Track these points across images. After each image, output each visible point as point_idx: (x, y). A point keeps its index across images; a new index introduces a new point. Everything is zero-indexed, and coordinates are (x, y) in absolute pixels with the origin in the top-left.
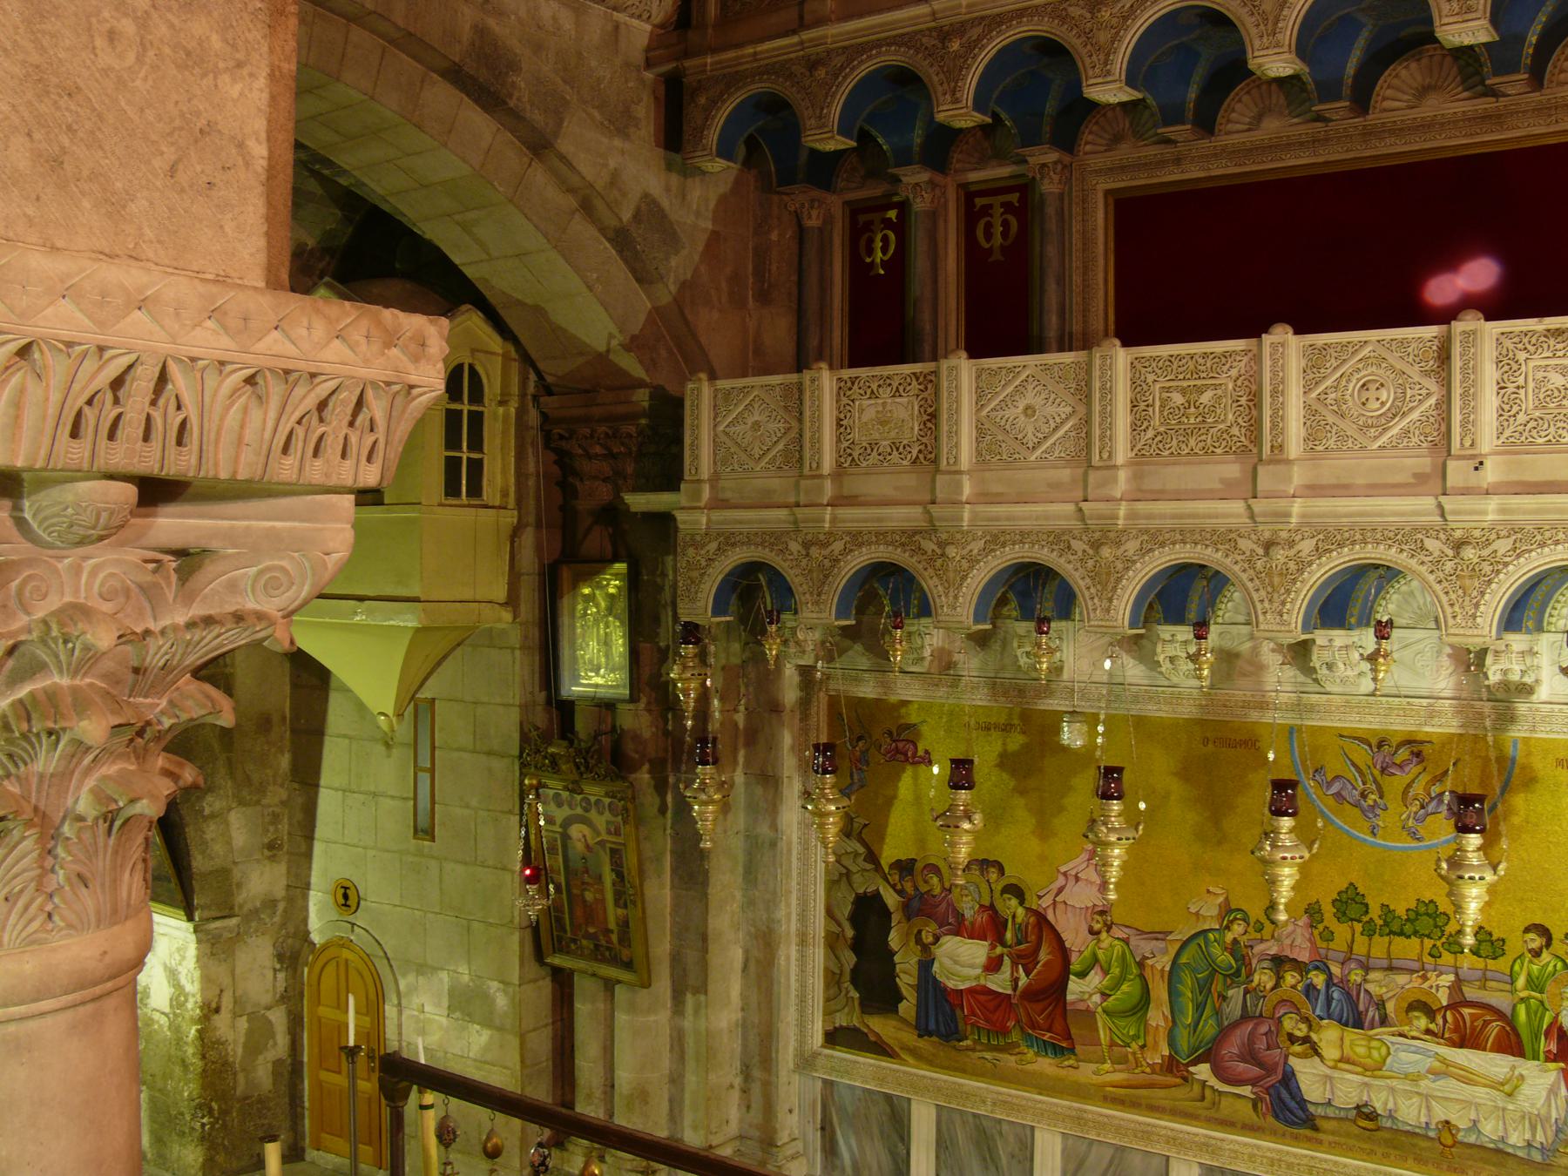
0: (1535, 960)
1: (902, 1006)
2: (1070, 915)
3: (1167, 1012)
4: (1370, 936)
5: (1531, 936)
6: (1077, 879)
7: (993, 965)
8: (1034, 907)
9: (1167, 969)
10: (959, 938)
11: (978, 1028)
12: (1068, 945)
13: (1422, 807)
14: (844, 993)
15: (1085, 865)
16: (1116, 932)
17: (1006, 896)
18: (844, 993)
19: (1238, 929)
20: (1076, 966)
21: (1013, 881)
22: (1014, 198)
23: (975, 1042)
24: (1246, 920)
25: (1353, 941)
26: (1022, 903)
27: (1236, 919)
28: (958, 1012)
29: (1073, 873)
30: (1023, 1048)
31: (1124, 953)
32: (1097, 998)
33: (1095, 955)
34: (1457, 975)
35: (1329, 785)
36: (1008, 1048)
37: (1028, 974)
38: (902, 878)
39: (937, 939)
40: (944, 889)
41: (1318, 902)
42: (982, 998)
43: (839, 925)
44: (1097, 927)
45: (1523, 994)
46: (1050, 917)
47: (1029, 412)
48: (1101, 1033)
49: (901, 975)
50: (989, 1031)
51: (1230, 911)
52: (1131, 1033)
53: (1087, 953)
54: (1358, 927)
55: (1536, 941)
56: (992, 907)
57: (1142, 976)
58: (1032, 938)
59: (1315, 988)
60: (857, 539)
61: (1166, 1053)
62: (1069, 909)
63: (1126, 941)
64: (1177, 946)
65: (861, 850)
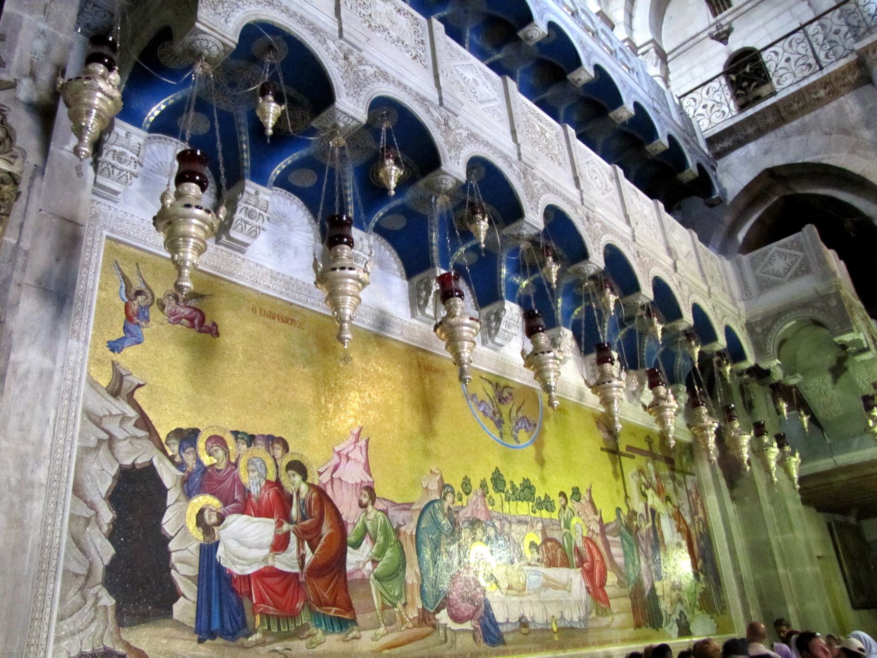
1: (178, 607)
2: (344, 490)
3: (418, 570)
4: (509, 501)
6: (348, 459)
7: (280, 544)
8: (316, 483)
9: (414, 533)
10: (245, 517)
11: (268, 616)
12: (344, 518)
14: (90, 602)
15: (352, 447)
16: (379, 505)
17: (291, 472)
18: (90, 602)
19: (449, 498)
20: (351, 538)
21: (296, 458)
23: (264, 633)
26: (305, 479)
28: (247, 604)
29: (345, 452)
30: (313, 630)
31: (385, 521)
32: (369, 566)
33: (365, 526)
36: (296, 635)
37: (313, 550)
38: (182, 448)
39: (221, 518)
40: (229, 463)
42: (269, 581)
43: (91, 506)
44: (365, 500)
46: (329, 492)
48: (375, 598)
49: (178, 566)
50: (278, 617)
52: (396, 594)
53: (359, 525)
56: (278, 483)
57: (398, 541)
58: (316, 513)
61: (420, 606)
62: (344, 484)
63: (385, 512)
64: (418, 514)
65: (132, 413)
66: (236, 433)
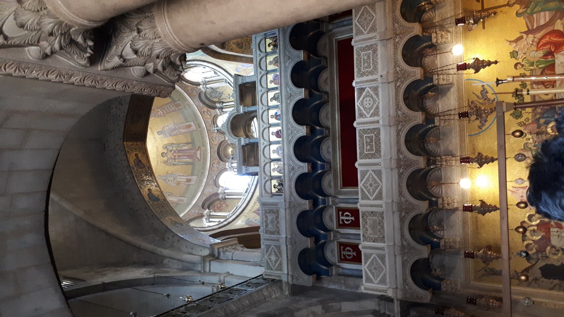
0: (525, 65)
5: (518, 67)
13: (486, 99)
22: (340, 213)
24: (527, 143)
25: (527, 113)
27: (527, 146)
29: (520, 198)
34: (533, 84)
35: (483, 124)
41: (517, 123)
45: (535, 66)
47: (371, 185)
51: (524, 148)
54: (523, 112)
55: (519, 66)
59: (545, 121)
60: (402, 236)
66: (523, 241)
